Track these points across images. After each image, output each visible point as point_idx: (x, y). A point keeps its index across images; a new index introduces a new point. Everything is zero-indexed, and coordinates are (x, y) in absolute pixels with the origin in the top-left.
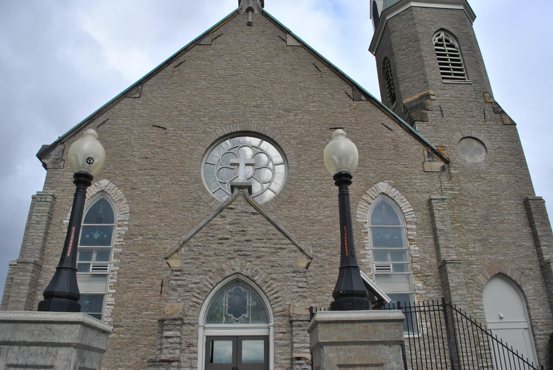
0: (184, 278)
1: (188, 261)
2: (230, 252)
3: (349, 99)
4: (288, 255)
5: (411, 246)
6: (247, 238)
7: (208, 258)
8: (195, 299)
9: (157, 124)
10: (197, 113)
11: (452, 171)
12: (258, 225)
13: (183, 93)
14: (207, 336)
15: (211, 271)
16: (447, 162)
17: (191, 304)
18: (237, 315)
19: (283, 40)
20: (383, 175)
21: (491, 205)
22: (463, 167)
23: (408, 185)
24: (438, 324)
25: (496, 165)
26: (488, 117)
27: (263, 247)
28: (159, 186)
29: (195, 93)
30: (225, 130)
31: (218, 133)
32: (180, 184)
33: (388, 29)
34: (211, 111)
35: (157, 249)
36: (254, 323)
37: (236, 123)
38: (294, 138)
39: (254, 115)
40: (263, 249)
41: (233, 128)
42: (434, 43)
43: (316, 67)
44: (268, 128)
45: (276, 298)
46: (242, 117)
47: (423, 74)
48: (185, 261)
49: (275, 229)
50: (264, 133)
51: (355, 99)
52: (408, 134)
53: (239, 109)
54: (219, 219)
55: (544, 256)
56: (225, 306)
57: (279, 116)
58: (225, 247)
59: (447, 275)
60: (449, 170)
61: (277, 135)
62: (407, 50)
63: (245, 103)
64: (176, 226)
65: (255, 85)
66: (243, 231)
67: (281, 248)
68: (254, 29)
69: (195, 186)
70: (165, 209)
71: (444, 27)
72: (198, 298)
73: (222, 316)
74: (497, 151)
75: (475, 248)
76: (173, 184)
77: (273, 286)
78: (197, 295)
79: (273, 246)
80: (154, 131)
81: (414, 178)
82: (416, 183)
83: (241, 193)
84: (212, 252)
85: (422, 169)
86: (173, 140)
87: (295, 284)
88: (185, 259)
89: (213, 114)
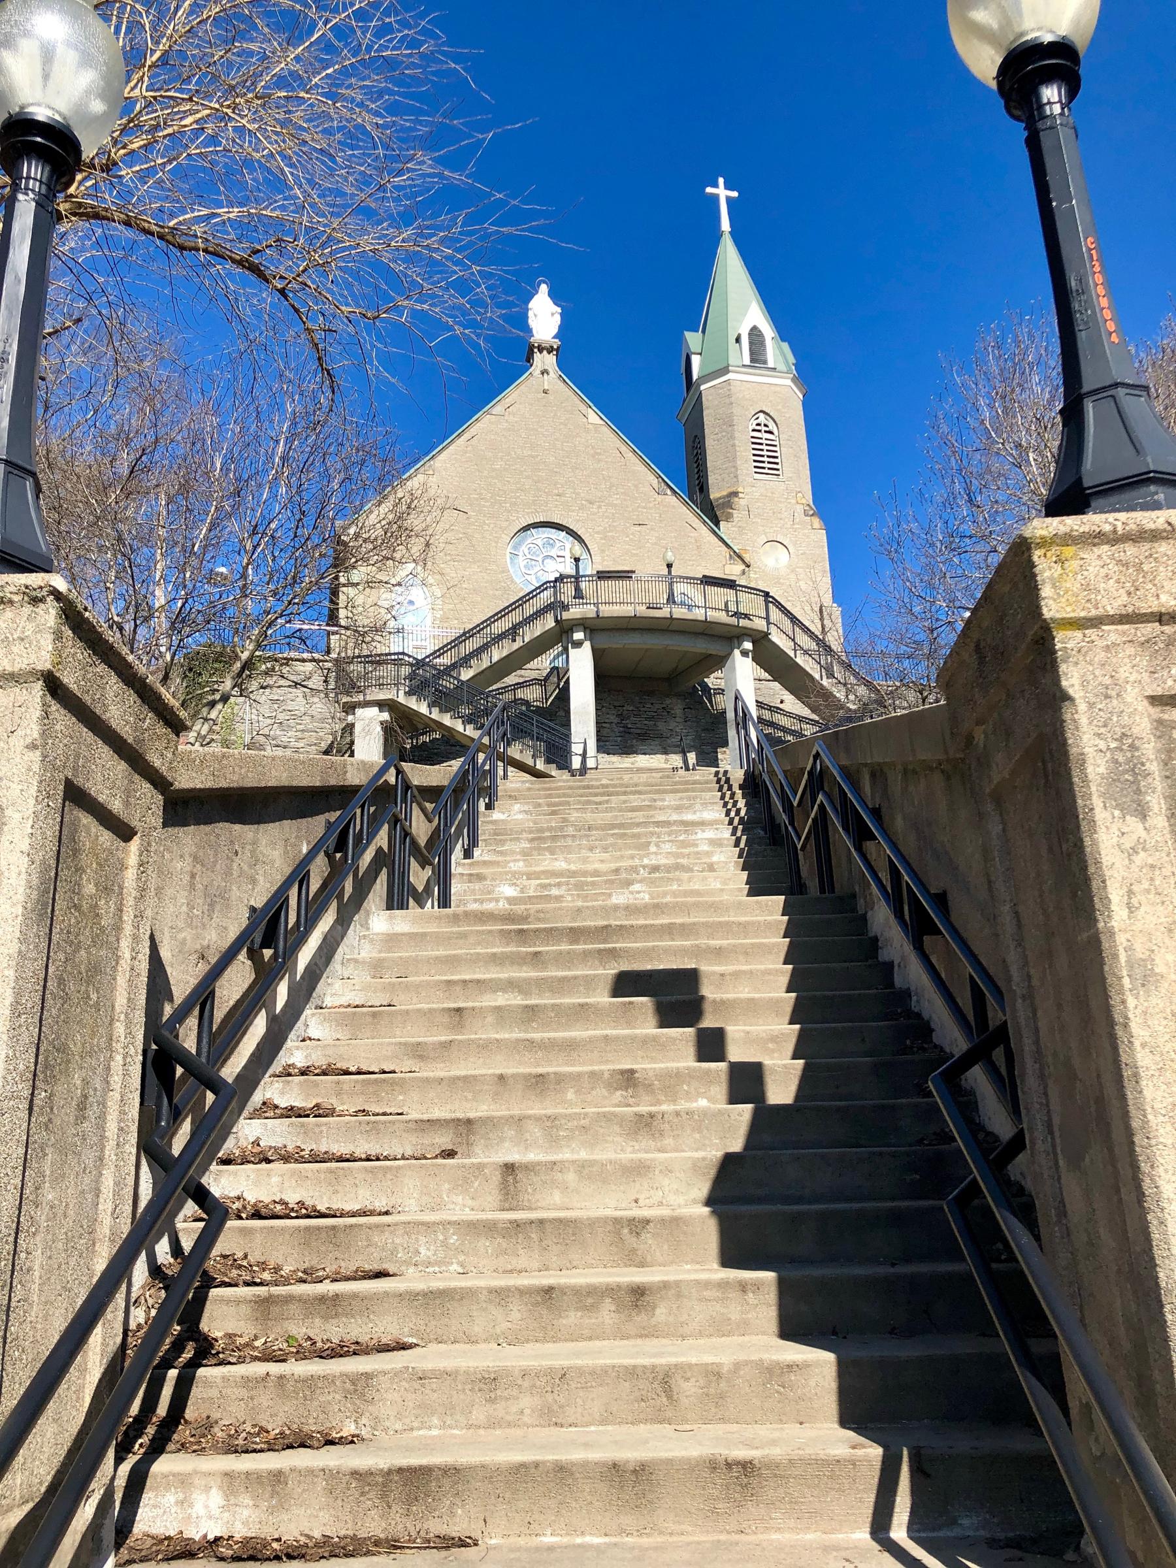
29: (494, 474)
38: (598, 533)
42: (751, 428)
57: (582, 508)
68: (551, 397)
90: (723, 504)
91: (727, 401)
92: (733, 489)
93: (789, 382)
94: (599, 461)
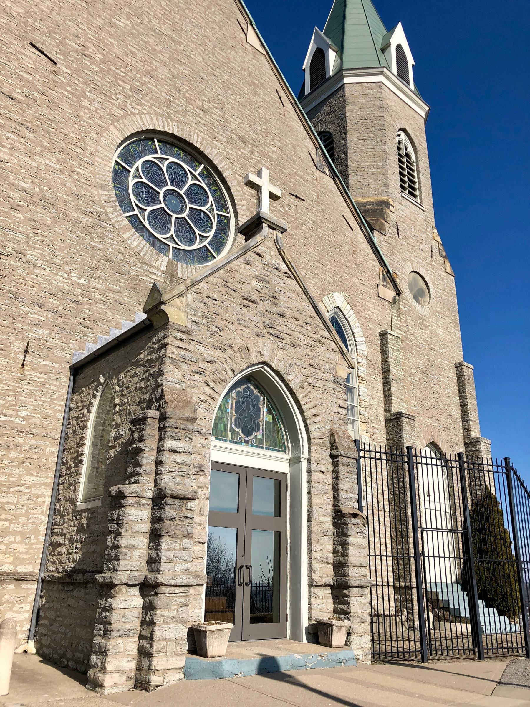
0: (190, 348)
1: (199, 320)
2: (258, 325)
3: (311, 164)
4: (327, 355)
5: (360, 385)
6: (280, 309)
7: (227, 324)
8: (208, 390)
9: (38, 45)
10: (112, 67)
11: (401, 307)
12: (293, 295)
13: (90, 18)
14: (212, 462)
15: (232, 347)
16: (399, 294)
17: (203, 397)
18: (247, 432)
19: (243, 30)
20: (340, 284)
21: (429, 360)
22: (411, 306)
23: (362, 307)
24: (380, 492)
25: (436, 316)
26: (434, 257)
27: (300, 333)
28: (35, 164)
29: (112, 30)
30: (155, 121)
31: (145, 121)
32: (76, 177)
33: (343, 96)
34: (136, 77)
35: (22, 281)
36: (269, 449)
37: (172, 120)
39: (199, 122)
40: (299, 335)
41: (168, 125)
43: (280, 98)
44: (216, 152)
45: (316, 415)
46: (182, 115)
47: (383, 174)
48: (193, 319)
49: (313, 309)
50: (210, 156)
51: (319, 168)
52: (366, 242)
53: (178, 100)
54: (243, 265)
55: (472, 433)
56: (232, 413)
58: (250, 313)
59: (402, 432)
60: (399, 304)
61: (228, 169)
62: (367, 136)
63: (187, 95)
64: (61, 249)
65: (201, 74)
66: (274, 297)
67: (319, 342)
69: (101, 192)
70: (44, 211)
71: (407, 128)
72: (212, 389)
73: (226, 429)
74: (439, 299)
75: (415, 406)
76: (60, 171)
77: (312, 396)
78: (212, 384)
79: (311, 335)
80: (32, 55)
81: (369, 301)
82: (370, 308)
83: (271, 236)
84: (233, 317)
85: (376, 292)
86: (67, 91)
87: (336, 400)
88: (193, 315)
89: (138, 84)
90: (373, 211)
91: (378, 103)
92: (385, 199)
93: (423, 115)
94: (256, 94)
